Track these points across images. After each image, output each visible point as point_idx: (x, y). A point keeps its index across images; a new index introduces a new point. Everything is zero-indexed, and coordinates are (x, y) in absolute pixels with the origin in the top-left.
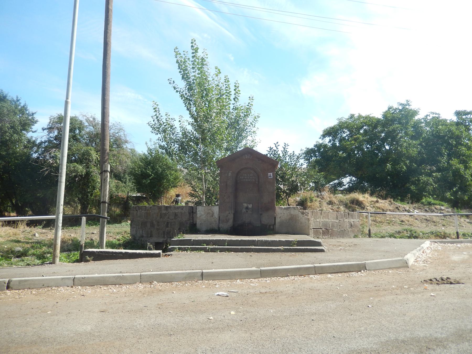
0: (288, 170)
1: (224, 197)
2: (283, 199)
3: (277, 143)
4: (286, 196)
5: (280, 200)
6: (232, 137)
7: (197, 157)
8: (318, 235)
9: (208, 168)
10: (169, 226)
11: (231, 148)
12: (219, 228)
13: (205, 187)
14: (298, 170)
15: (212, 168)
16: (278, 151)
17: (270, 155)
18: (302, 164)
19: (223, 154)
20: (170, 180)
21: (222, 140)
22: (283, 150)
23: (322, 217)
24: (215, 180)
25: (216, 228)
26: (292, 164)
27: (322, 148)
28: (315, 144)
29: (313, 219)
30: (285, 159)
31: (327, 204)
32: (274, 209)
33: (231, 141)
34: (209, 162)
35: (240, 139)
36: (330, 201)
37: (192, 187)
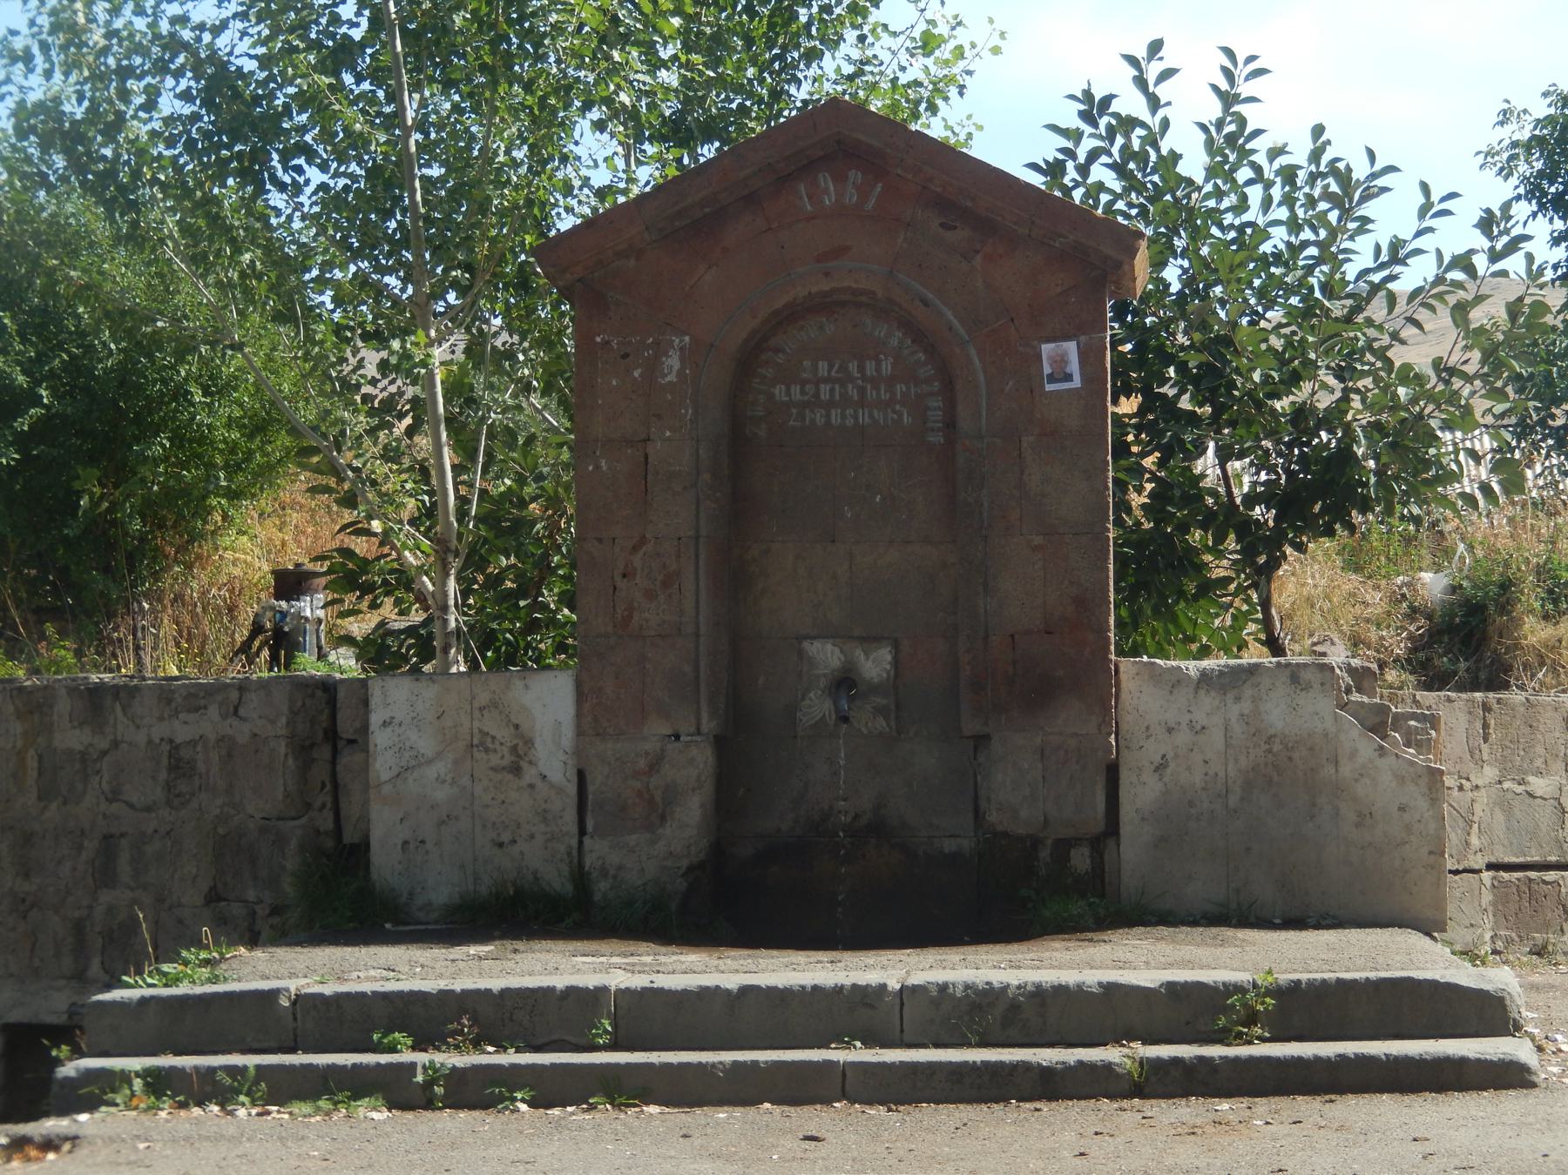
1: (621, 584)
12: (580, 877)
14: (1357, 309)
18: (1396, 245)
25: (557, 880)
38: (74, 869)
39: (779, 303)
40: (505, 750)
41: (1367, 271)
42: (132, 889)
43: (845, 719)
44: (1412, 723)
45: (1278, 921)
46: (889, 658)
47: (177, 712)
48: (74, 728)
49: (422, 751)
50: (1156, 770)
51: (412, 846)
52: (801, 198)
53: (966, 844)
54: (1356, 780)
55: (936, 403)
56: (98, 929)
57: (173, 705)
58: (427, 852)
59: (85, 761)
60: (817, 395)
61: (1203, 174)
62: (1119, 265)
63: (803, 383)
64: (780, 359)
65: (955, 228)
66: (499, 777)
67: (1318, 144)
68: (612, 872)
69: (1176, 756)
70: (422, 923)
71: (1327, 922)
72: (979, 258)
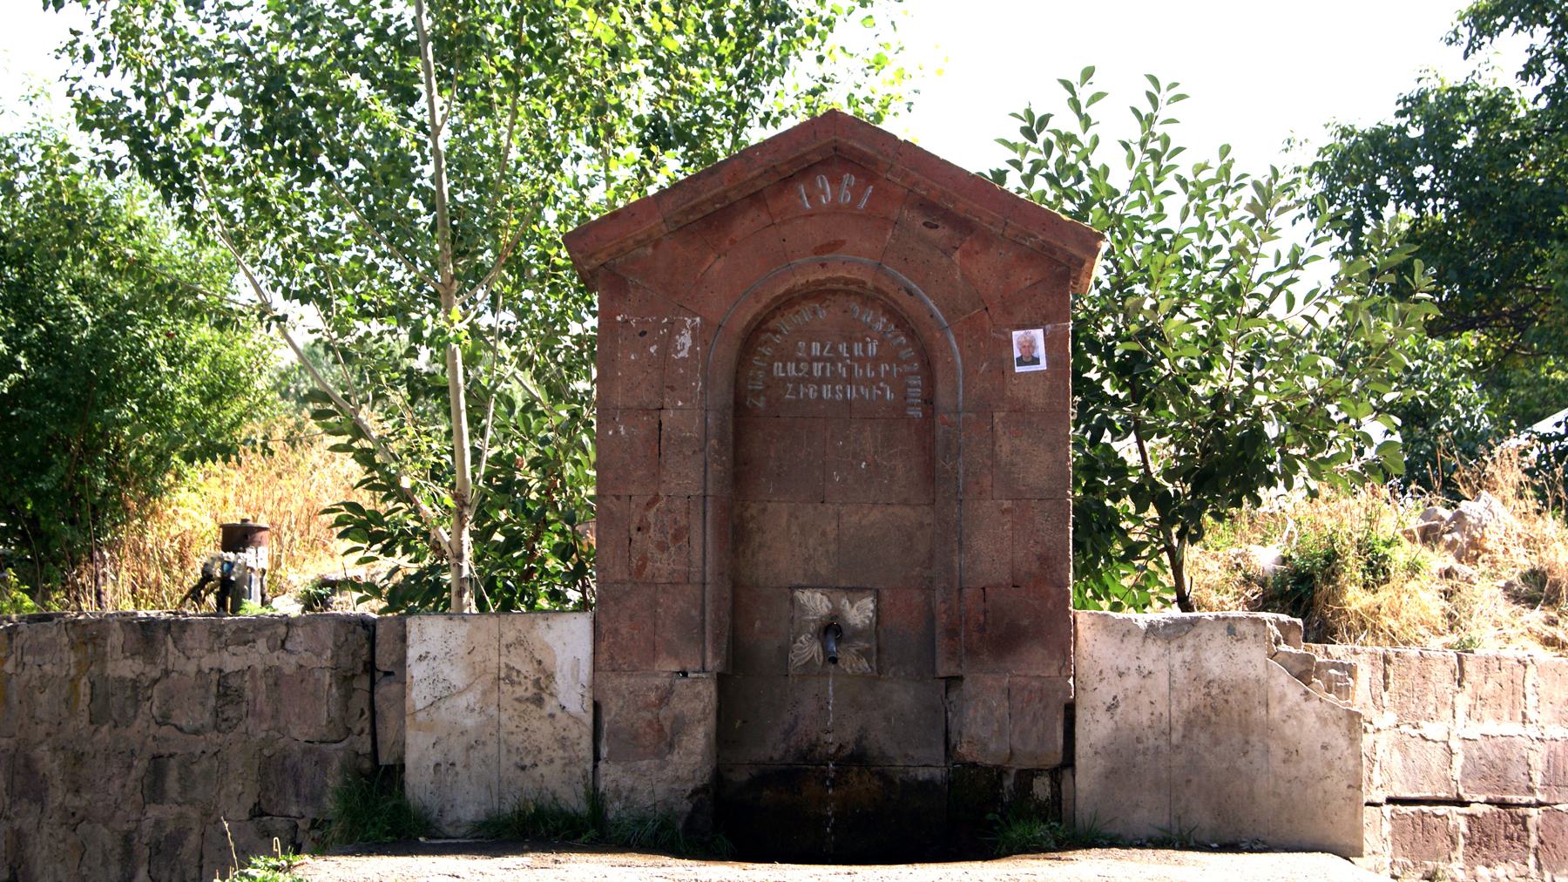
0: (1177, 309)
1: (637, 536)
2: (1133, 551)
3: (1088, 73)
4: (1165, 522)
5: (1109, 558)
6: (700, 29)
7: (402, 202)
8: (1436, 855)
9: (494, 297)
10: (172, 784)
11: (689, 124)
12: (596, 799)
13: (477, 454)
14: (1264, 307)
15: (528, 294)
16: (1096, 141)
17: (1028, 180)
18: (1296, 253)
19: (622, 173)
20: (167, 403)
21: (614, 53)
22: (1134, 133)
23: (1463, 701)
24: (557, 393)
25: (573, 799)
26: (1208, 253)
27: (1470, 123)
28: (1411, 89)
29: (1390, 718)
30: (1151, 210)
31: (1514, 596)
32: (1060, 638)
33: (690, 57)
34: (506, 237)
35: (773, 45)
36: (1534, 573)
37: (365, 457)
38: (124, 786)
39: (781, 290)
40: (529, 684)
41: (1269, 274)
42: (179, 805)
43: (834, 660)
44: (1333, 671)
45: (1215, 845)
46: (871, 606)
47: (227, 645)
48: (126, 658)
49: (454, 683)
50: (1109, 709)
51: (443, 768)
52: (801, 197)
53: (938, 773)
54: (1284, 721)
55: (916, 381)
56: (145, 840)
57: (223, 638)
58: (457, 774)
59: (135, 686)
60: (810, 372)
61: (1128, 186)
62: (1081, 263)
63: (798, 361)
64: (778, 339)
65: (937, 227)
66: (524, 707)
67: (1225, 161)
68: (625, 794)
69: (1126, 697)
70: (447, 838)
71: (1260, 846)
72: (957, 255)
